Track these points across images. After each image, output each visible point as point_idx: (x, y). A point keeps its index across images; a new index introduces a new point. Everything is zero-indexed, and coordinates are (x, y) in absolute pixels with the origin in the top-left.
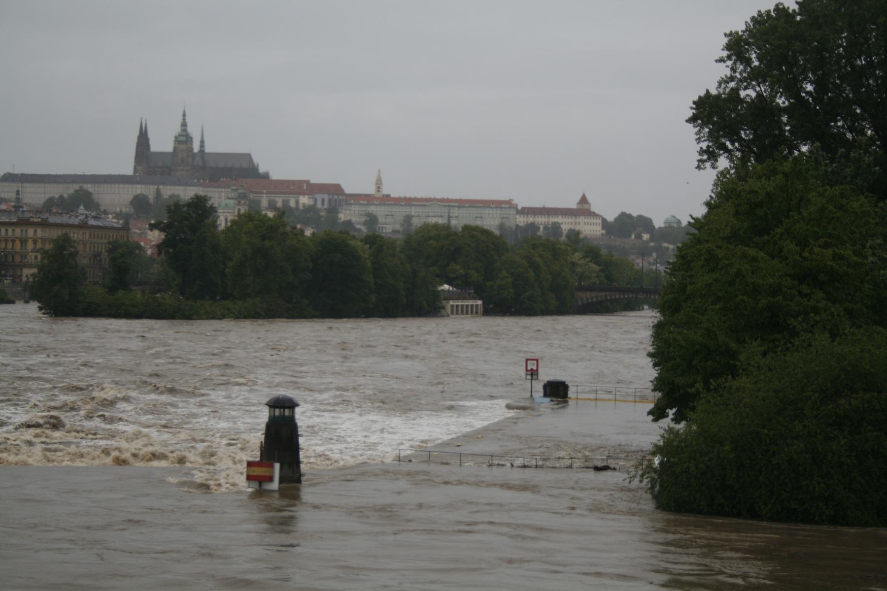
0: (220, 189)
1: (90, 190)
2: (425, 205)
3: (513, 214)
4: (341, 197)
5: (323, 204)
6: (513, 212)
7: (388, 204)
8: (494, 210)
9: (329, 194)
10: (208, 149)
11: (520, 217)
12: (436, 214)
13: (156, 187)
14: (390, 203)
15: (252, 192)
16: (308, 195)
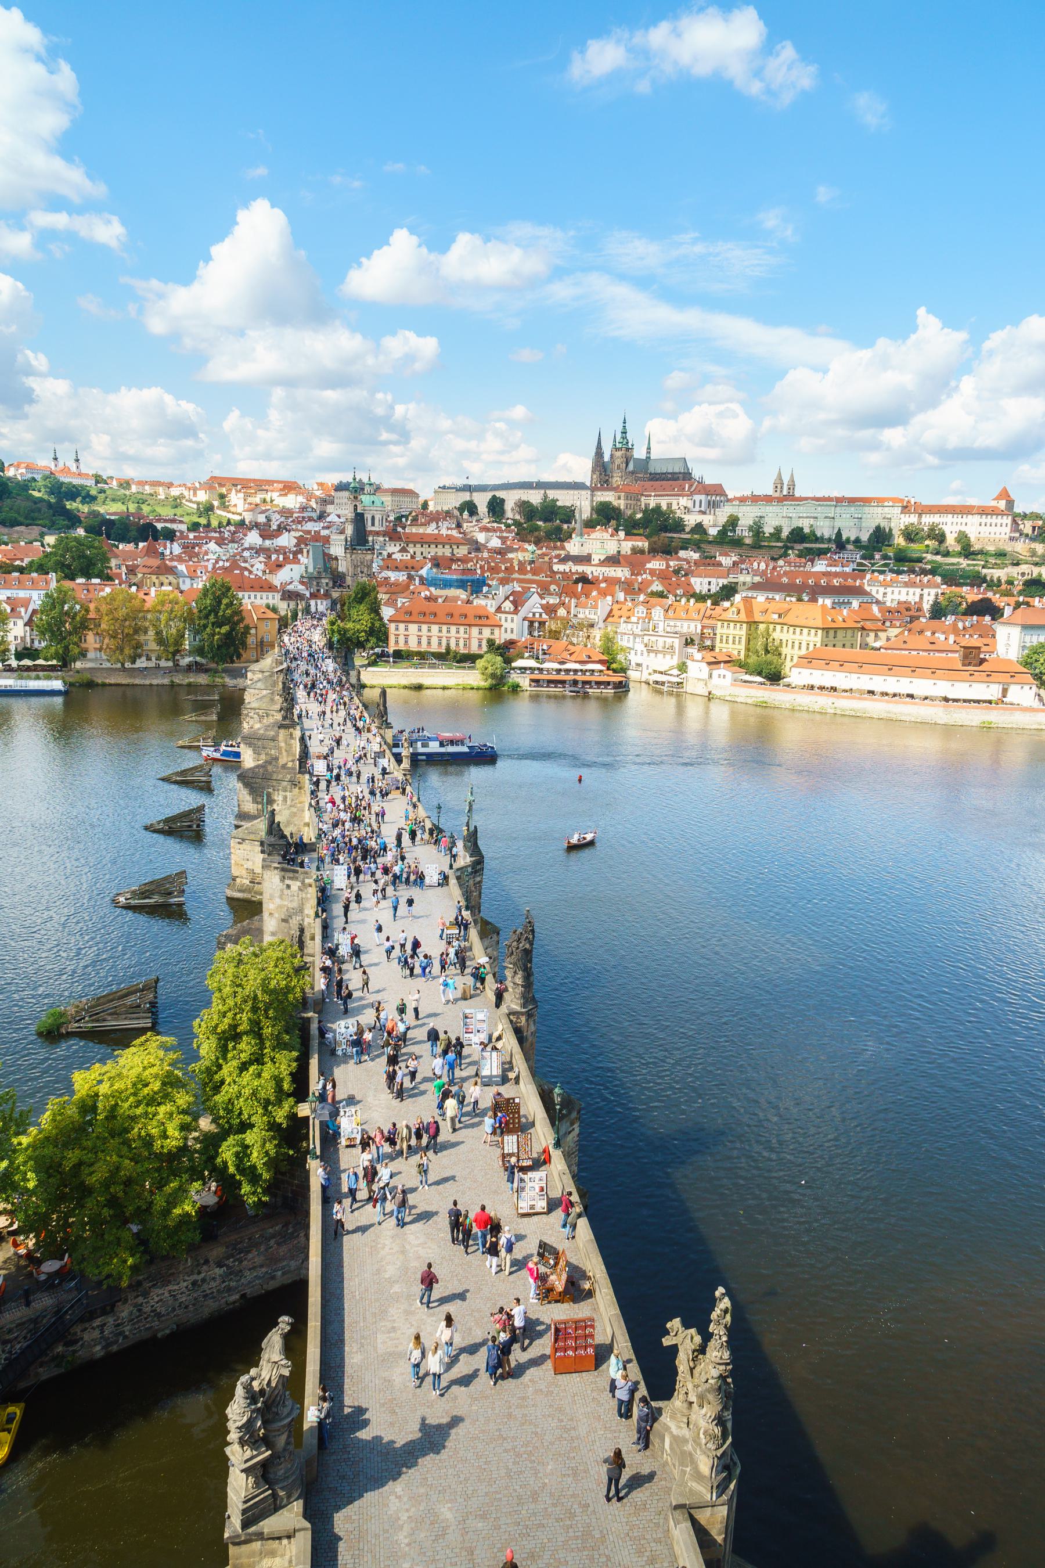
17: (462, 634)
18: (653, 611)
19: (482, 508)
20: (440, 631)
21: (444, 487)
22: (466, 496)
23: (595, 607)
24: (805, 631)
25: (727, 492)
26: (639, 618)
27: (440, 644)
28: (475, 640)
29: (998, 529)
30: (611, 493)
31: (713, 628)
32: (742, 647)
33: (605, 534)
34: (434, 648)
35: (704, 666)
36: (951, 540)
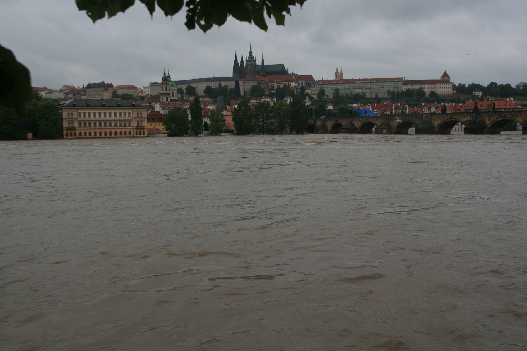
0: (254, 82)
1: (195, 86)
2: (353, 83)
3: (401, 85)
4: (311, 82)
6: (400, 83)
7: (333, 83)
8: (390, 83)
9: (305, 80)
10: (265, 64)
11: (404, 86)
12: (359, 87)
13: (219, 82)
14: (334, 83)
15: (270, 82)
16: (295, 81)
18: (431, 109)
21: (155, 83)
25: (315, 79)
29: (447, 90)
36: (427, 94)
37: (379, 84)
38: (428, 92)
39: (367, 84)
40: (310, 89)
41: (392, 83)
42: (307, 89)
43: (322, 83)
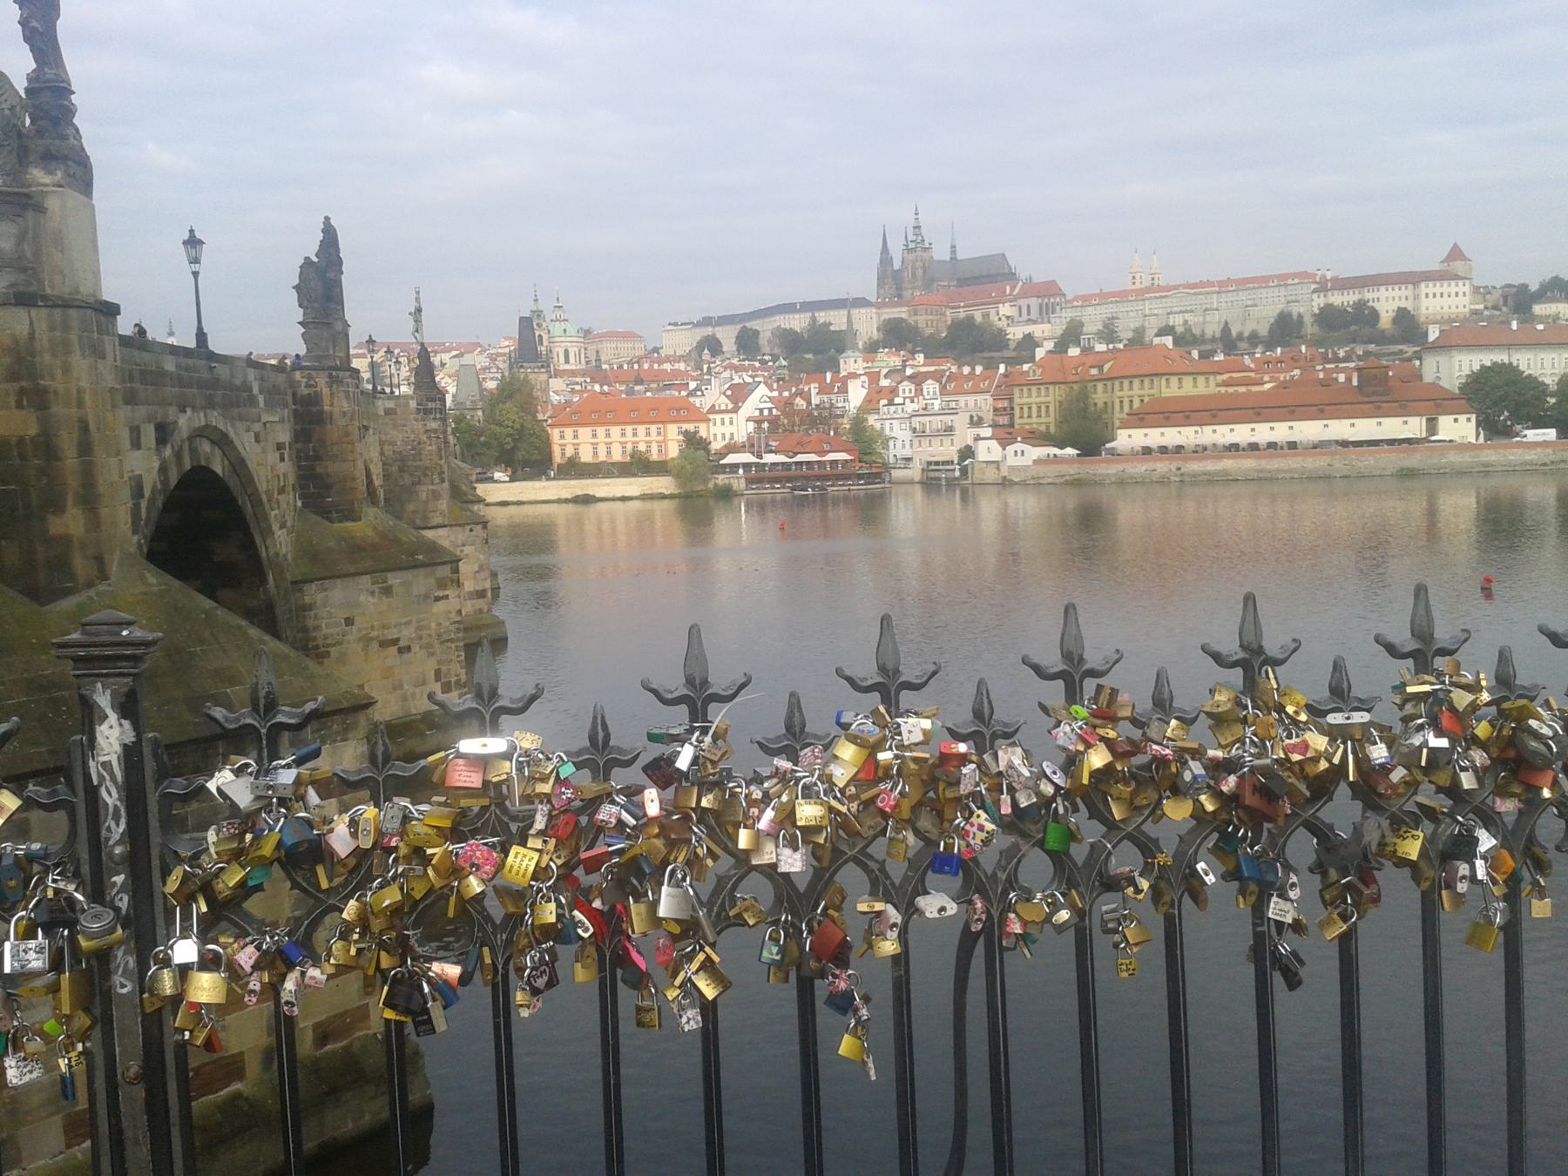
2: (1166, 296)
4: (1052, 300)
5: (1029, 314)
8: (1276, 290)
9: (1038, 297)
11: (1319, 297)
12: (1183, 309)
13: (810, 314)
15: (948, 307)
17: (654, 436)
18: (925, 386)
19: (729, 345)
20: (623, 435)
21: (675, 324)
22: (709, 331)
23: (844, 390)
24: (1136, 382)
26: (905, 398)
27: (624, 452)
28: (668, 442)
29: (1453, 301)
30: (904, 309)
31: (1011, 400)
32: (1051, 419)
33: (894, 358)
34: (617, 456)
35: (994, 444)
36: (1386, 320)
37: (1243, 296)
38: (1390, 311)
39: (1208, 296)
40: (1049, 322)
41: (1282, 289)
42: (1042, 323)
43: (1080, 303)
